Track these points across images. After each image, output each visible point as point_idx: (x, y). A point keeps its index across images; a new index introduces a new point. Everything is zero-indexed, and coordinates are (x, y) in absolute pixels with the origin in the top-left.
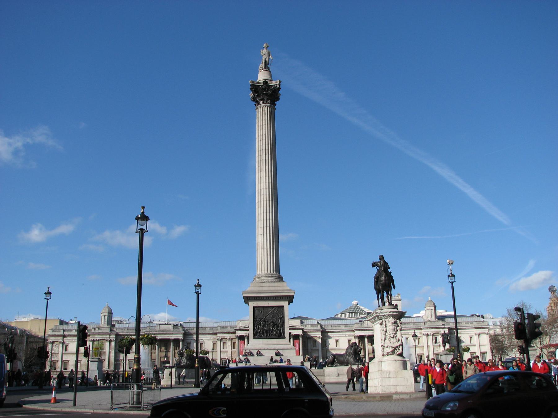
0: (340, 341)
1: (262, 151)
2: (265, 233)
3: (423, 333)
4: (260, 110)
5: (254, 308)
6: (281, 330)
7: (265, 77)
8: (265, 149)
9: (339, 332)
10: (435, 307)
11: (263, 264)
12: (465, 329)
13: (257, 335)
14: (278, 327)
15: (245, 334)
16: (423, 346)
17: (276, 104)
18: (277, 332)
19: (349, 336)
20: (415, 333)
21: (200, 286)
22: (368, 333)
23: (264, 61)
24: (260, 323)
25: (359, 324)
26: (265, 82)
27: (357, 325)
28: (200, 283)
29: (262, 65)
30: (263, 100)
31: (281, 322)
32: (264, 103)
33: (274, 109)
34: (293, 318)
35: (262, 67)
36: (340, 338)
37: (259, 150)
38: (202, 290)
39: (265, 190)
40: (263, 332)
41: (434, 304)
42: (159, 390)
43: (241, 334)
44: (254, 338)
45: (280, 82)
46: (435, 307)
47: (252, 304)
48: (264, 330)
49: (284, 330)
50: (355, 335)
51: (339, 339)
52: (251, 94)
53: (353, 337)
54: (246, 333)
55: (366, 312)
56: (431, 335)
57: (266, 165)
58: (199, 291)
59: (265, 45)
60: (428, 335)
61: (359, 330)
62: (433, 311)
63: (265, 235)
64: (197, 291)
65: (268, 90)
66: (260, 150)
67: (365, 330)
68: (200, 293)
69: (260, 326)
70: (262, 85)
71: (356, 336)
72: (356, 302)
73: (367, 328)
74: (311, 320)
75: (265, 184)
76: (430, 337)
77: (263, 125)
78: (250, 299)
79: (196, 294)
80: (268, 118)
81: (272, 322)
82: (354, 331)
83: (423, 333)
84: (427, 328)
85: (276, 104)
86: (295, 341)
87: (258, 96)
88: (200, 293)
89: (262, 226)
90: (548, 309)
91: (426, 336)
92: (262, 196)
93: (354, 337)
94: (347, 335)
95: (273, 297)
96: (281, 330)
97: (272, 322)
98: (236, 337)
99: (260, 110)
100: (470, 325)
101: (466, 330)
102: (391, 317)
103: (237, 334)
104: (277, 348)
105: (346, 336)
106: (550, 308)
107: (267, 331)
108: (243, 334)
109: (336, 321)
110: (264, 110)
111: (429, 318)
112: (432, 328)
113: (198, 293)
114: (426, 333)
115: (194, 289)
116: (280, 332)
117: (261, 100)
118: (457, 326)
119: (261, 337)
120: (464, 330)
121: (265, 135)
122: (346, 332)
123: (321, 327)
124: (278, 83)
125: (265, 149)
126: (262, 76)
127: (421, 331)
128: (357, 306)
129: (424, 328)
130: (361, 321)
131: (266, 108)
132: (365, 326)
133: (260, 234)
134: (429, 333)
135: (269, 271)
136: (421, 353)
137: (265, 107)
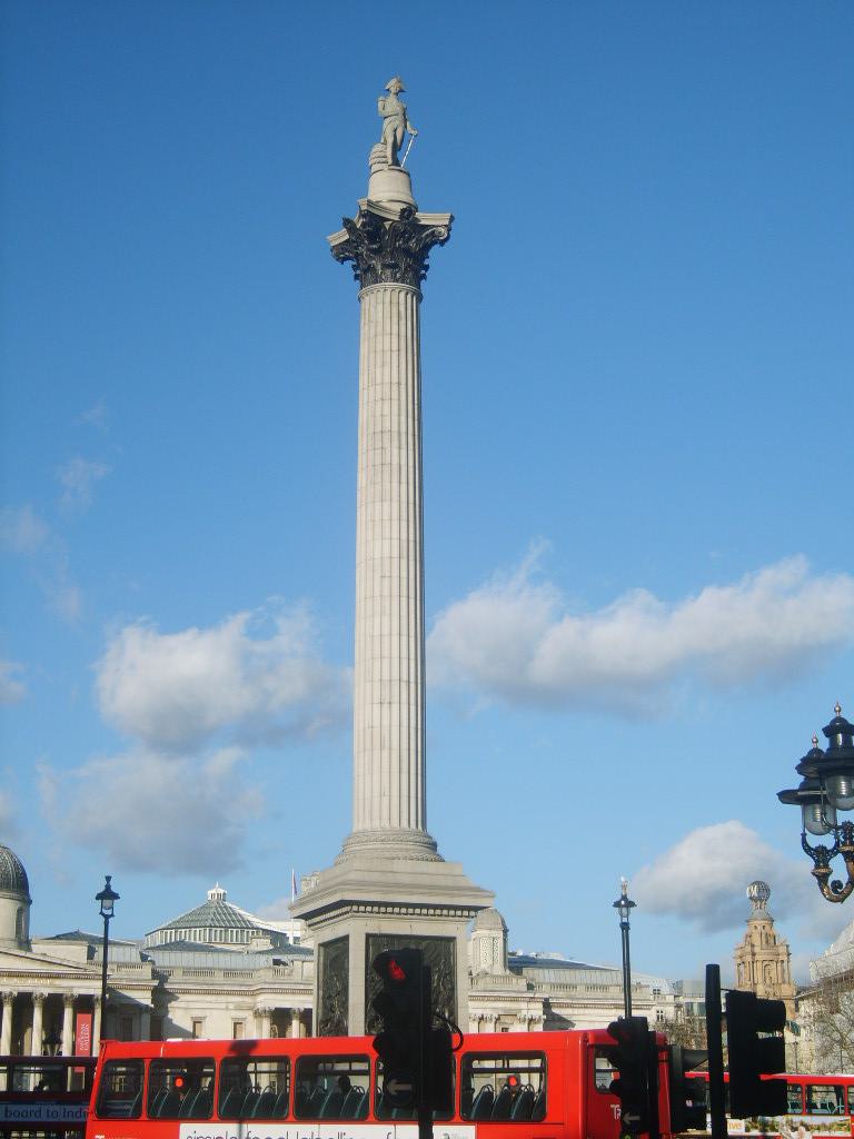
0: (206, 1023)
1: (387, 436)
2: (396, 699)
7: (398, 192)
8: (399, 432)
9: (208, 992)
10: (505, 931)
12: (586, 1006)
19: (239, 1008)
21: (630, 904)
22: (304, 1002)
23: (390, 140)
25: (271, 973)
26: (408, 212)
29: (382, 150)
31: (445, 988)
33: (420, 298)
34: (58, 937)
36: (207, 1013)
38: (635, 917)
39: (396, 561)
41: (503, 922)
45: (452, 219)
46: (505, 931)
51: (205, 1018)
52: (342, 236)
53: (251, 1013)
55: (258, 928)
59: (393, 85)
61: (275, 991)
63: (395, 707)
65: (410, 239)
67: (293, 992)
70: (397, 218)
72: (222, 891)
73: (302, 987)
74: (121, 949)
75: (396, 543)
80: (406, 328)
82: (253, 994)
86: (78, 1015)
90: (739, 953)
94: (231, 1006)
100: (599, 994)
101: (587, 1011)
102: (291, 942)
105: (227, 1008)
106: (748, 949)
109: (197, 954)
110: (395, 300)
111: (484, 966)
112: (498, 999)
114: (479, 1013)
115: (615, 918)
117: (385, 266)
118: (630, 996)
120: (581, 1011)
121: (399, 384)
122: (229, 993)
123: (155, 974)
124: (447, 223)
125: (399, 432)
126: (386, 190)
128: (225, 907)
130: (277, 962)
131: (409, 296)
132: (297, 977)
133: (377, 700)
134: (487, 1013)
135: (405, 823)
137: (407, 294)
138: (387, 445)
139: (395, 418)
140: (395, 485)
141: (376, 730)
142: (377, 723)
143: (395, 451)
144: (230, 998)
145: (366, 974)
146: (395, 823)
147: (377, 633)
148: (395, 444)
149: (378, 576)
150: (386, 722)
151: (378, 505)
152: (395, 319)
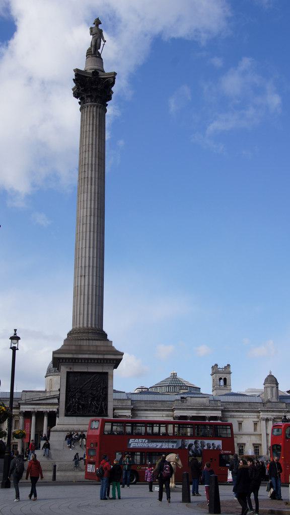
1: (86, 166)
2: (87, 274)
3: (261, 416)
4: (86, 111)
5: (68, 373)
6: (103, 405)
9: (155, 410)
11: (82, 315)
13: (70, 412)
14: (98, 400)
15: (32, 410)
16: (261, 435)
17: (107, 105)
18: (97, 408)
20: (285, 416)
24: (75, 395)
27: (177, 402)
28: (18, 335)
30: (90, 96)
32: (91, 102)
35: (91, 52)
37: (83, 164)
40: (78, 406)
42: (148, 486)
43: (27, 410)
44: (66, 415)
47: (64, 369)
48: (80, 404)
49: (106, 405)
50: (175, 415)
54: (33, 408)
56: (271, 420)
57: (91, 185)
58: (16, 345)
60: (267, 420)
62: (274, 389)
63: (87, 277)
64: (13, 345)
66: (85, 164)
67: (187, 409)
68: (18, 349)
69: (75, 398)
71: (176, 417)
76: (271, 423)
77: (89, 131)
78: (63, 362)
79: (11, 350)
81: (91, 394)
83: (261, 416)
84: (267, 411)
85: (107, 105)
87: (85, 91)
88: (18, 349)
89: (83, 265)
91: (265, 422)
92: (85, 226)
93: (174, 418)
95: (94, 359)
96: (103, 405)
97: (91, 394)
98: (20, 413)
99: (86, 111)
103: (21, 410)
104: (70, 429)
107: (83, 406)
108: (29, 410)
110: (92, 110)
112: (273, 411)
113: (14, 349)
114: (266, 417)
116: (101, 407)
117: (87, 97)
119: (76, 414)
122: (163, 410)
123: (132, 404)
124: (113, 76)
127: (258, 414)
129: (263, 411)
131: (95, 108)
132: (188, 404)
133: (79, 275)
134: (269, 417)
136: (258, 442)
138: (86, 170)
139: (90, 159)
140: (89, 186)
141: (79, 287)
142: (79, 285)
143: (90, 172)
144: (164, 412)
145: (66, 387)
146: (85, 325)
147: (80, 247)
148: (90, 169)
149: (81, 224)
150: (83, 284)
151: (82, 195)
152: (91, 118)
